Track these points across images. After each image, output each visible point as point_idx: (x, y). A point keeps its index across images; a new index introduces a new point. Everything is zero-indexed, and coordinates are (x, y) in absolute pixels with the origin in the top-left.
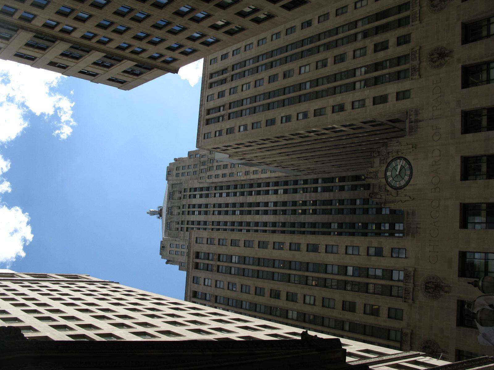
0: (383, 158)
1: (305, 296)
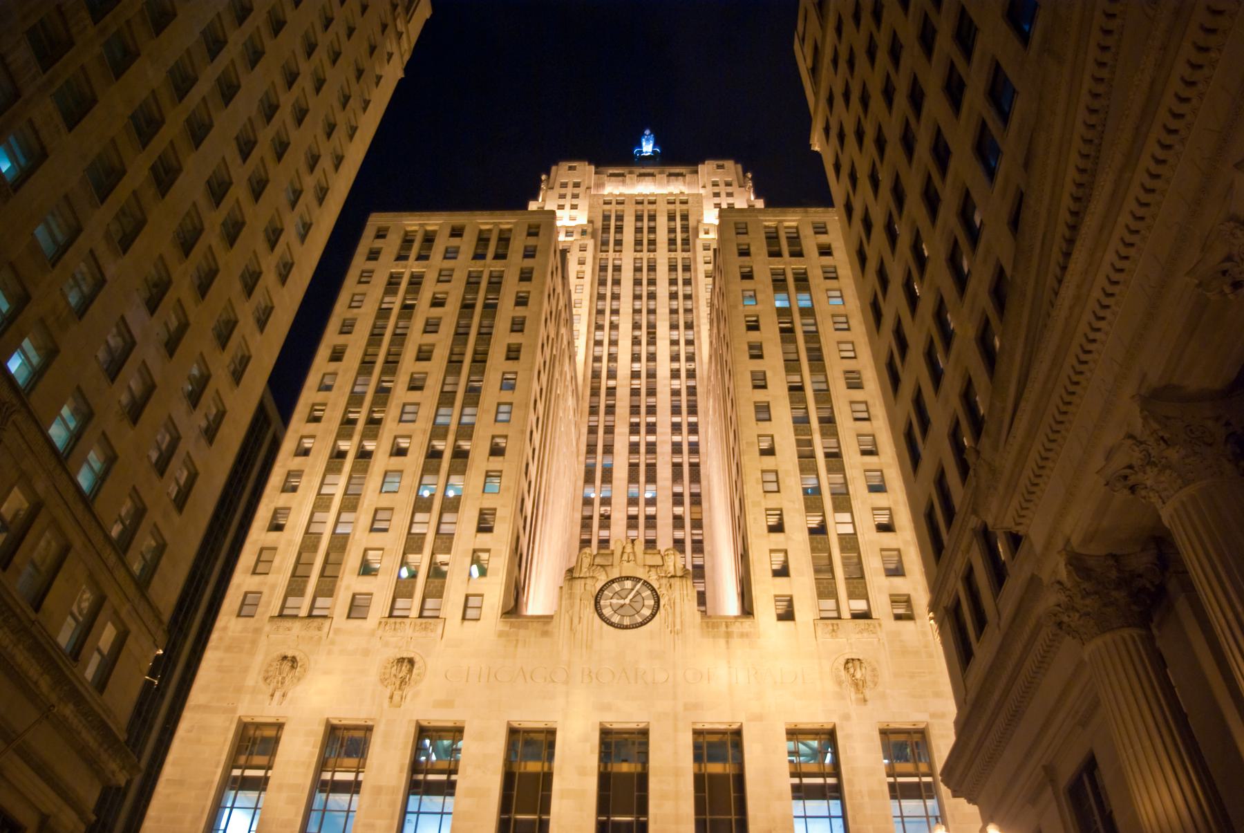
1: (410, 437)
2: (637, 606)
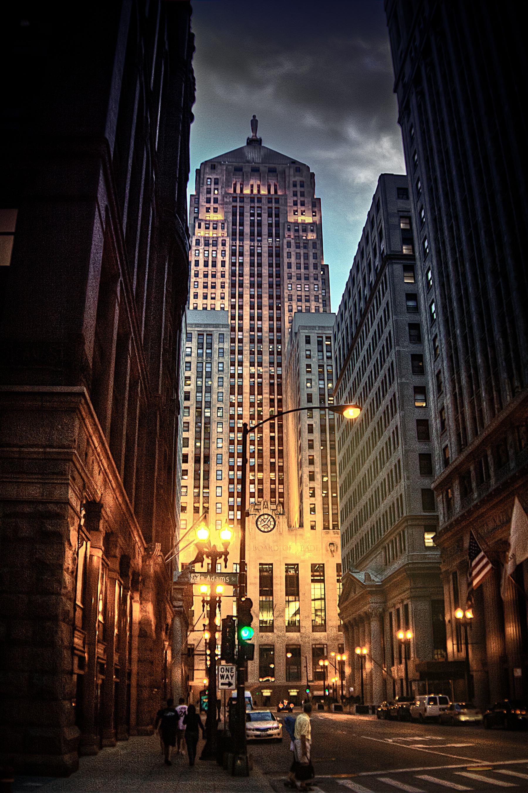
2: (269, 524)
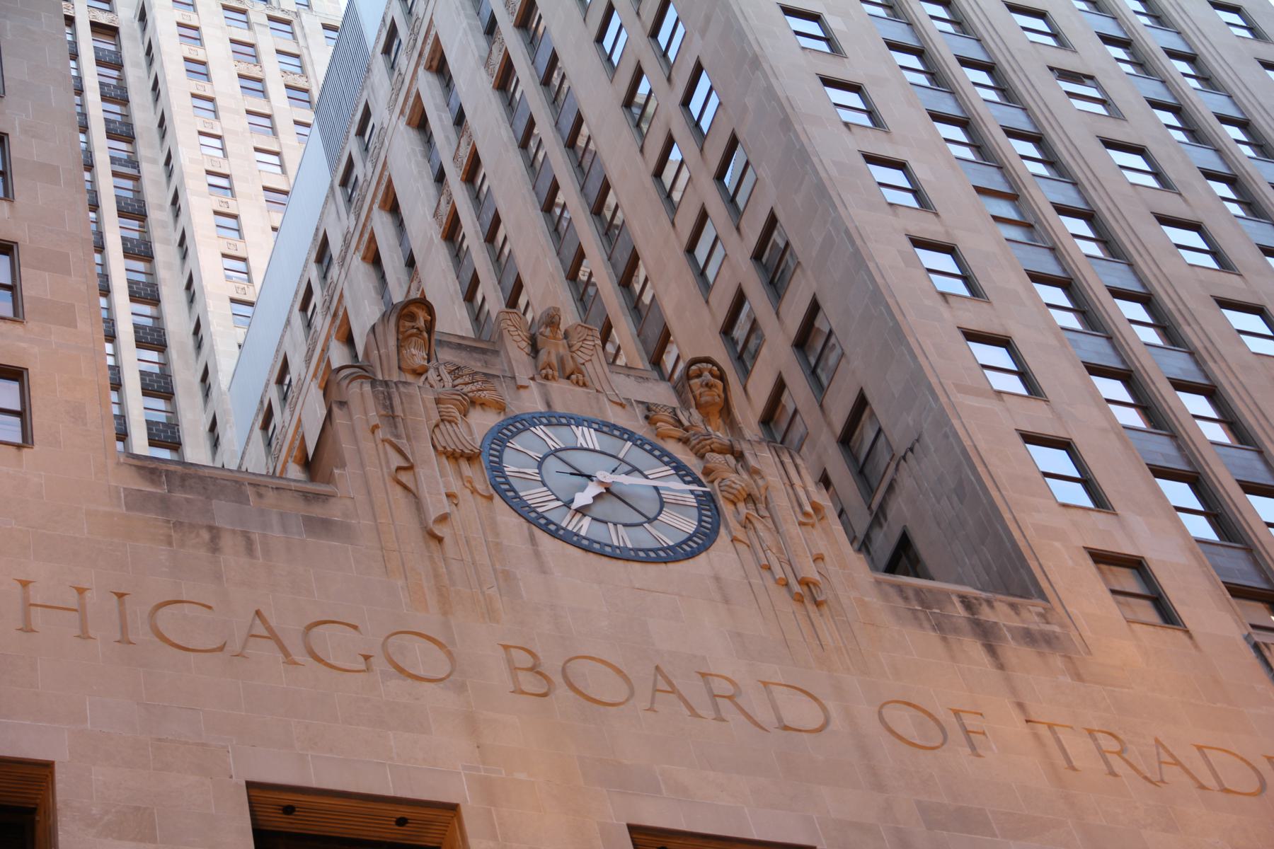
0: (686, 423)
